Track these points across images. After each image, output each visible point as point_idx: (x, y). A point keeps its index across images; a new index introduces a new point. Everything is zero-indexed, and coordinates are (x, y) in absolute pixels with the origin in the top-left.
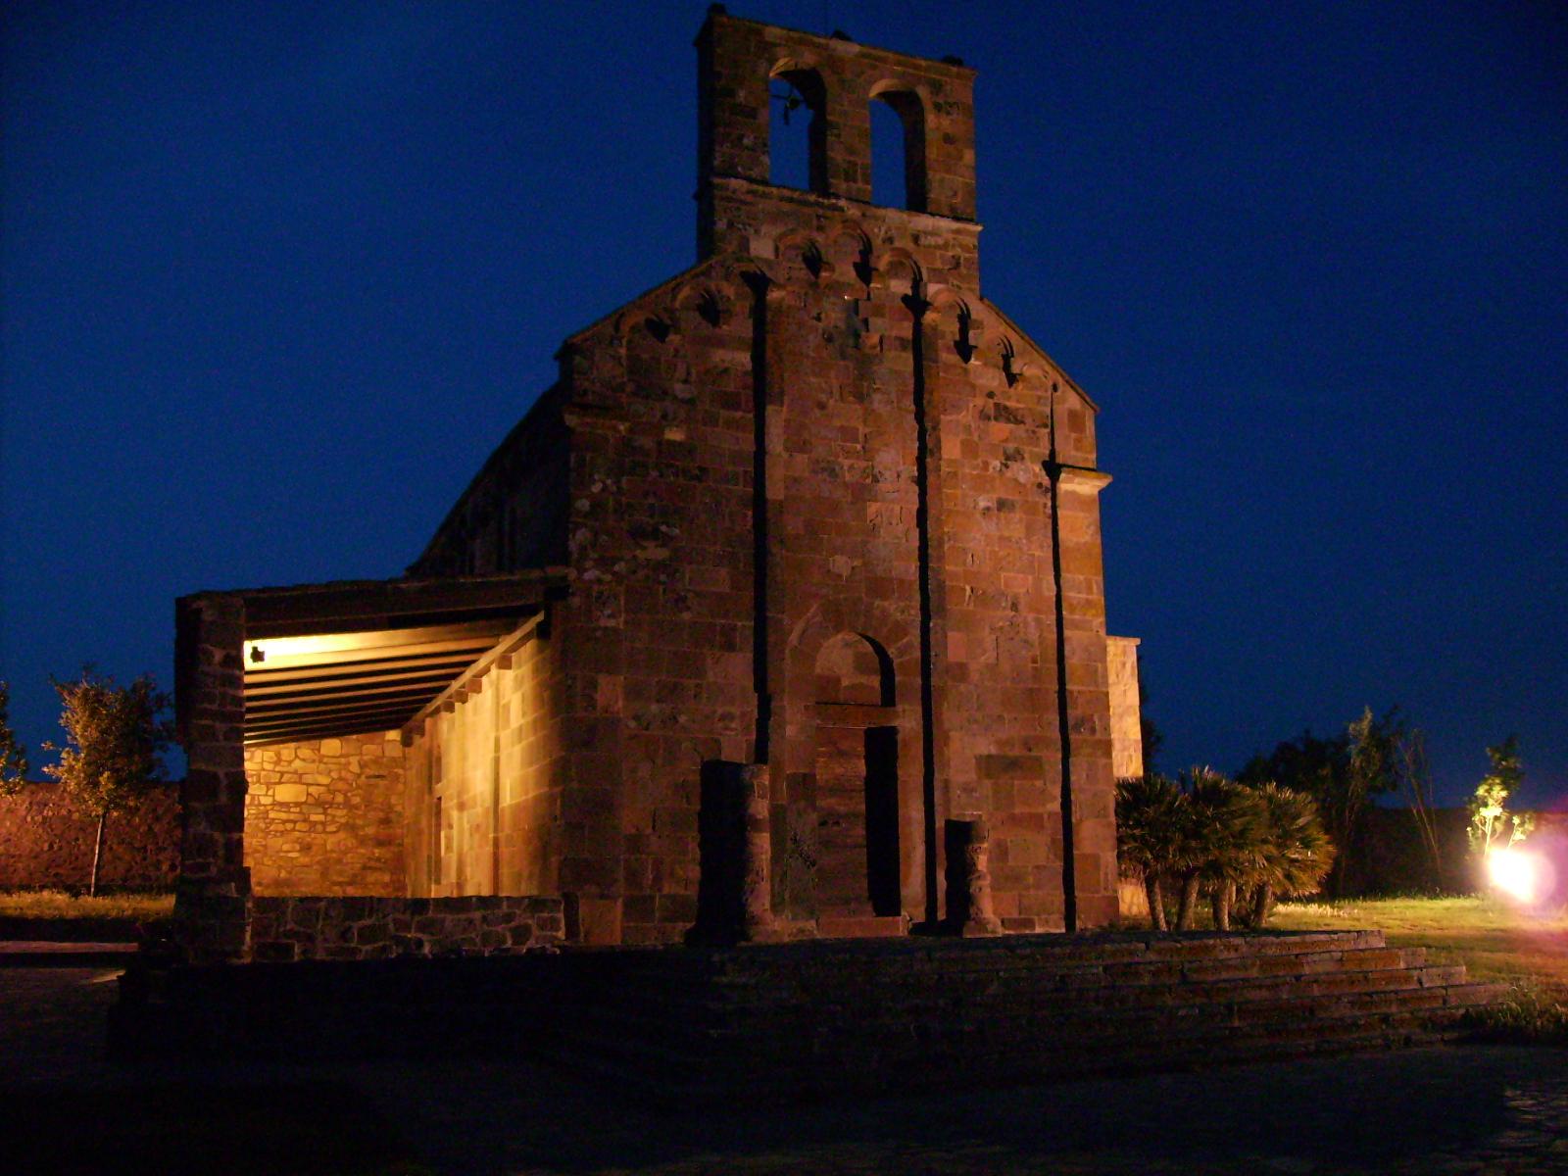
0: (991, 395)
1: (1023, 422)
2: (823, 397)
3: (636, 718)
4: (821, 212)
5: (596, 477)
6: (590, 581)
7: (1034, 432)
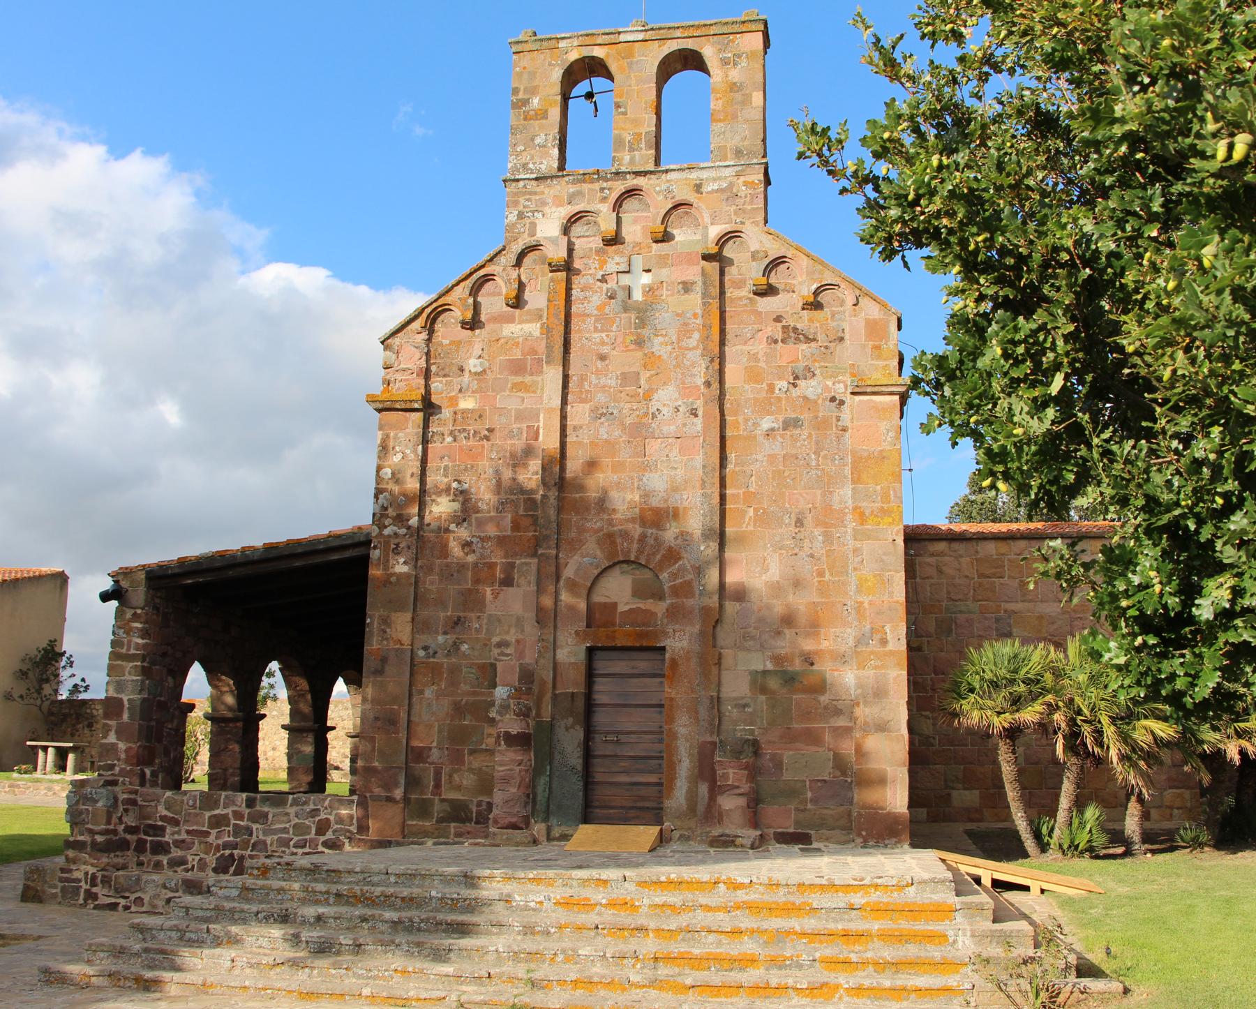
0: (778, 319)
1: (814, 340)
2: (605, 350)
3: (425, 648)
4: (605, 185)
5: (398, 449)
6: (389, 536)
7: (826, 347)
